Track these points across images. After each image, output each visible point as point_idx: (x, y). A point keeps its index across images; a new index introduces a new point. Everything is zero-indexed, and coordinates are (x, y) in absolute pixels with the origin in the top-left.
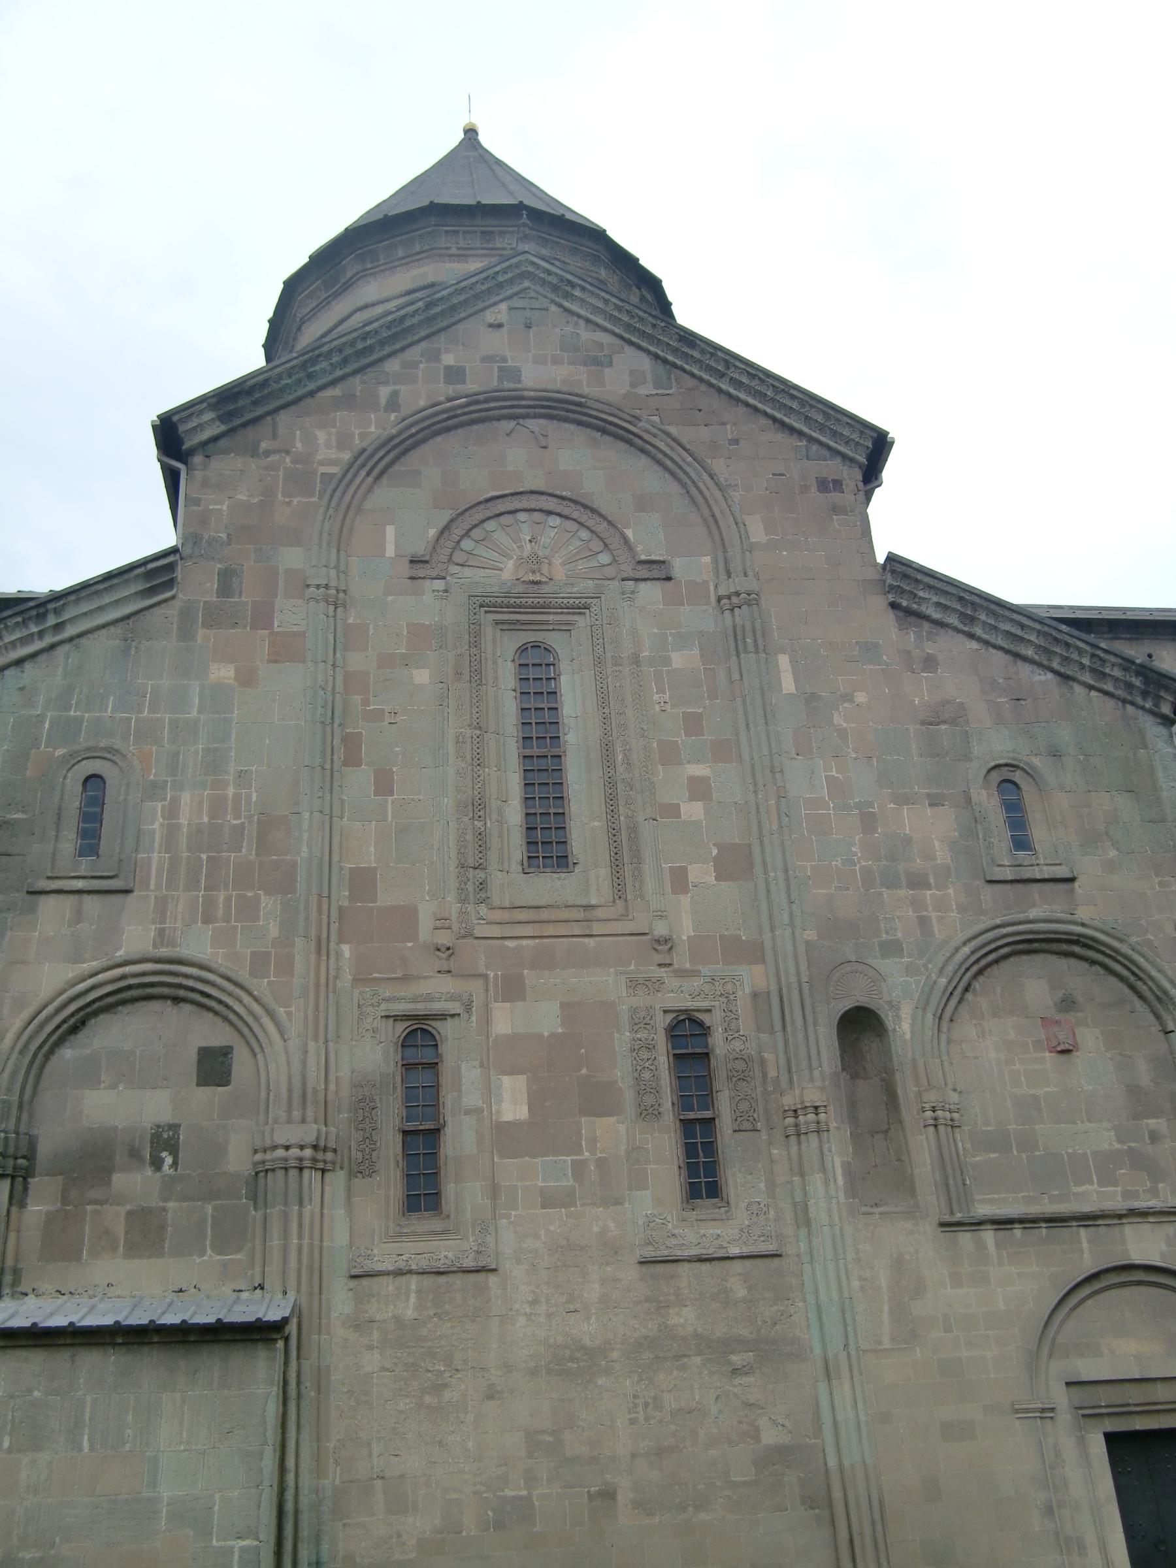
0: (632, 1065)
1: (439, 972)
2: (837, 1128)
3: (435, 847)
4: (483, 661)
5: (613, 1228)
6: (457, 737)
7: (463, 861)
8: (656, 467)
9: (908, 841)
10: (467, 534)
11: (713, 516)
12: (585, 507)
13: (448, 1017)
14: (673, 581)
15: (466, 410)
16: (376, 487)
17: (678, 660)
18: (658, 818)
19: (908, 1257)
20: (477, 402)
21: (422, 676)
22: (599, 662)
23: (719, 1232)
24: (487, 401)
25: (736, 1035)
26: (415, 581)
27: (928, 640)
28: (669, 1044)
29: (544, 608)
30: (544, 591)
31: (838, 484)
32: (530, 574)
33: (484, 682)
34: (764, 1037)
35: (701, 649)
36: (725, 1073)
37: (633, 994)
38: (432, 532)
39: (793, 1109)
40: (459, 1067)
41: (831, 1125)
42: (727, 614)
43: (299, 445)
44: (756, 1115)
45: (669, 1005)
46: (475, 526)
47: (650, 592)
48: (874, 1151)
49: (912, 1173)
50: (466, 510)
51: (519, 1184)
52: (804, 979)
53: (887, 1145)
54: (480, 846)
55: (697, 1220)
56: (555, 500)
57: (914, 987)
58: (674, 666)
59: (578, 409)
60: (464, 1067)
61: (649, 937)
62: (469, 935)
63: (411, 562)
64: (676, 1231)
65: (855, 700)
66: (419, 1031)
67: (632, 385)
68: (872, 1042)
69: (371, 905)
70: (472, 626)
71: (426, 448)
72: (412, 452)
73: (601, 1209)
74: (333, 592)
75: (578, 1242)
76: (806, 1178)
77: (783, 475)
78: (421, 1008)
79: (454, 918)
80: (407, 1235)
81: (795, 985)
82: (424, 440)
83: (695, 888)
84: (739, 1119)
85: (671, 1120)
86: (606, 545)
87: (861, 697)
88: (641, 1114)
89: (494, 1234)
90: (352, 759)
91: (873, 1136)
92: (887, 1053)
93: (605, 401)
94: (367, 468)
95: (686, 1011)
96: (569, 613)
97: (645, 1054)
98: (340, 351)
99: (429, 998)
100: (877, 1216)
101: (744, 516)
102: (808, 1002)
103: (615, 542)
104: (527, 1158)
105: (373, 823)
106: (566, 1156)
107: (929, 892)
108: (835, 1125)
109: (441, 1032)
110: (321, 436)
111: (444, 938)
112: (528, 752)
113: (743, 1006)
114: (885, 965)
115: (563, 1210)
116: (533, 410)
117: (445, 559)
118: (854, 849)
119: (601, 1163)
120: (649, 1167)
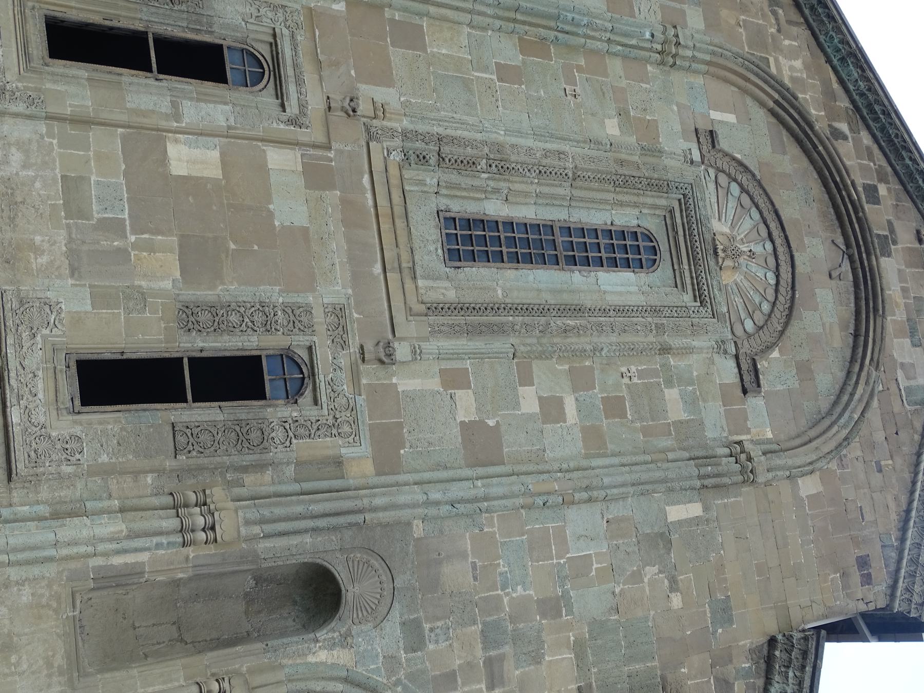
0: (244, 302)
1: (328, 98)
2: (187, 558)
3: (455, 115)
4: (636, 191)
5: (39, 260)
6: (563, 153)
7: (445, 140)
8: (837, 387)
9: (537, 659)
10: (743, 190)
11: (810, 441)
12: (791, 308)
13: (280, 101)
14: (743, 395)
15: (847, 200)
16: (765, 110)
17: (672, 394)
18: (516, 360)
19: (13, 659)
20: (856, 213)
21: (612, 128)
22: (655, 310)
23: (41, 395)
24: (858, 219)
25: (291, 434)
26: (694, 134)
27: (746, 684)
28: (271, 352)
29: (693, 259)
30: (709, 260)
31: (867, 579)
32: (722, 247)
33: (617, 189)
34: (290, 471)
35: (687, 421)
36: (243, 416)
37: (327, 310)
38: (739, 156)
39: (208, 500)
40: (226, 103)
41: (191, 549)
42: (727, 451)
43: (787, 42)
44: (194, 453)
45: (319, 353)
46: (752, 198)
47: (727, 371)
48: (154, 625)
49: (132, 668)
50: (764, 190)
51: (91, 153)
52: (368, 517)
53: (164, 642)
54: (462, 162)
55: (55, 368)
56: (790, 280)
57: (372, 667)
58: (666, 391)
59: (871, 310)
60: (228, 108)
61: (390, 336)
62: (371, 136)
63: (711, 132)
64: (39, 338)
65: (674, 594)
66: (261, 70)
67: (902, 364)
68: (294, 620)
69: (389, 40)
70: (666, 183)
71: (805, 162)
72: (799, 149)
73: (64, 248)
74: (674, 51)
75: (20, 214)
76: (119, 515)
77: (863, 519)
78: (288, 71)
79: (385, 123)
80: (22, 13)
81: (359, 504)
82: (812, 161)
83: (449, 396)
84: (188, 432)
85: (182, 345)
86: (761, 328)
87: (676, 601)
88: (187, 307)
89: (28, 112)
90: (526, 47)
91: (174, 623)
92: (283, 634)
93: (884, 334)
94: (781, 100)
95: (314, 375)
96: (693, 284)
97: (259, 318)
98: (869, 90)
99: (299, 82)
100: (71, 614)
101: (818, 473)
102: (341, 520)
103: (766, 336)
104: (123, 167)
105: (470, 57)
106: (129, 214)
107: (483, 686)
108: (192, 555)
109: (262, 93)
110: (798, 64)
111: (364, 108)
112: (557, 231)
113: (325, 445)
114: (393, 628)
115: (61, 202)
116: (859, 266)
117: (719, 164)
118: (519, 588)
119: (123, 254)
120: (122, 311)
